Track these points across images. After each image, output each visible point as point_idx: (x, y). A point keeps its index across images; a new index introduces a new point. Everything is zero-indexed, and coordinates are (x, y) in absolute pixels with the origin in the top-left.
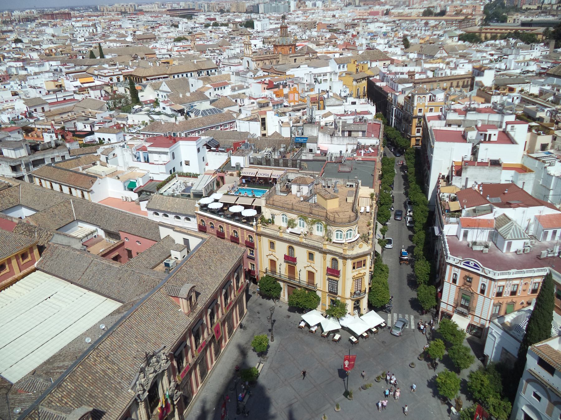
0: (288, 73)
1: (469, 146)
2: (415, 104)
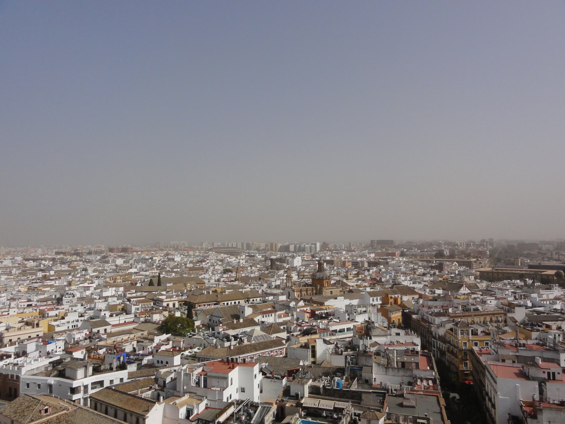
0: (326, 303)
1: (536, 385)
2: (460, 336)
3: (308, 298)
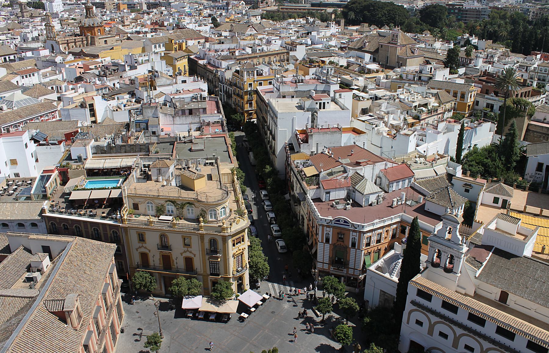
1: (309, 114)
3: (78, 50)
